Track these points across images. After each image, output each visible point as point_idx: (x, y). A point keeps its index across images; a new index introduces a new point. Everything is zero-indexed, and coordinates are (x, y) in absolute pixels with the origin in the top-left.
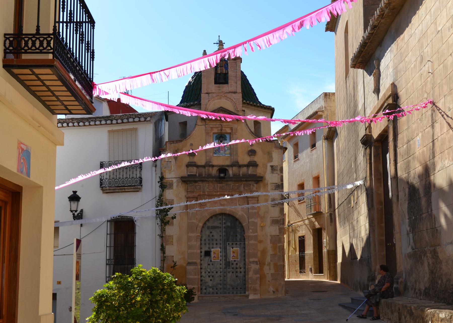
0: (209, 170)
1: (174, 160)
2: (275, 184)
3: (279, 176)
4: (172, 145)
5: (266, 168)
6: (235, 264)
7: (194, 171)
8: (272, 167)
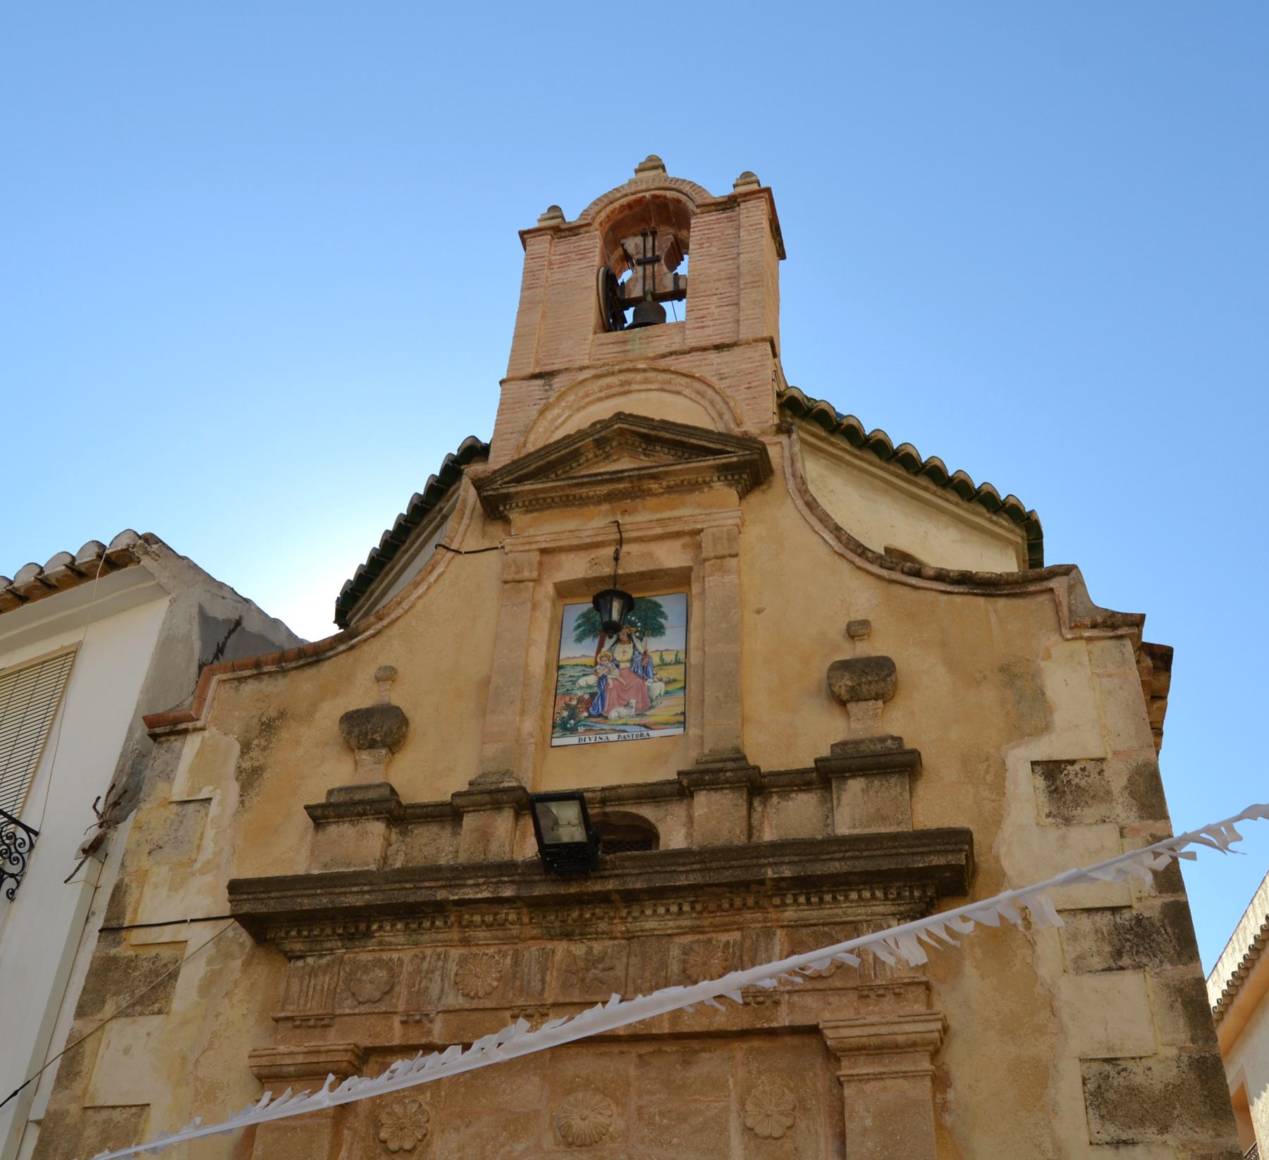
0: (485, 836)
1: (235, 787)
2: (1104, 921)
4: (250, 688)
5: (999, 787)
8: (1051, 770)
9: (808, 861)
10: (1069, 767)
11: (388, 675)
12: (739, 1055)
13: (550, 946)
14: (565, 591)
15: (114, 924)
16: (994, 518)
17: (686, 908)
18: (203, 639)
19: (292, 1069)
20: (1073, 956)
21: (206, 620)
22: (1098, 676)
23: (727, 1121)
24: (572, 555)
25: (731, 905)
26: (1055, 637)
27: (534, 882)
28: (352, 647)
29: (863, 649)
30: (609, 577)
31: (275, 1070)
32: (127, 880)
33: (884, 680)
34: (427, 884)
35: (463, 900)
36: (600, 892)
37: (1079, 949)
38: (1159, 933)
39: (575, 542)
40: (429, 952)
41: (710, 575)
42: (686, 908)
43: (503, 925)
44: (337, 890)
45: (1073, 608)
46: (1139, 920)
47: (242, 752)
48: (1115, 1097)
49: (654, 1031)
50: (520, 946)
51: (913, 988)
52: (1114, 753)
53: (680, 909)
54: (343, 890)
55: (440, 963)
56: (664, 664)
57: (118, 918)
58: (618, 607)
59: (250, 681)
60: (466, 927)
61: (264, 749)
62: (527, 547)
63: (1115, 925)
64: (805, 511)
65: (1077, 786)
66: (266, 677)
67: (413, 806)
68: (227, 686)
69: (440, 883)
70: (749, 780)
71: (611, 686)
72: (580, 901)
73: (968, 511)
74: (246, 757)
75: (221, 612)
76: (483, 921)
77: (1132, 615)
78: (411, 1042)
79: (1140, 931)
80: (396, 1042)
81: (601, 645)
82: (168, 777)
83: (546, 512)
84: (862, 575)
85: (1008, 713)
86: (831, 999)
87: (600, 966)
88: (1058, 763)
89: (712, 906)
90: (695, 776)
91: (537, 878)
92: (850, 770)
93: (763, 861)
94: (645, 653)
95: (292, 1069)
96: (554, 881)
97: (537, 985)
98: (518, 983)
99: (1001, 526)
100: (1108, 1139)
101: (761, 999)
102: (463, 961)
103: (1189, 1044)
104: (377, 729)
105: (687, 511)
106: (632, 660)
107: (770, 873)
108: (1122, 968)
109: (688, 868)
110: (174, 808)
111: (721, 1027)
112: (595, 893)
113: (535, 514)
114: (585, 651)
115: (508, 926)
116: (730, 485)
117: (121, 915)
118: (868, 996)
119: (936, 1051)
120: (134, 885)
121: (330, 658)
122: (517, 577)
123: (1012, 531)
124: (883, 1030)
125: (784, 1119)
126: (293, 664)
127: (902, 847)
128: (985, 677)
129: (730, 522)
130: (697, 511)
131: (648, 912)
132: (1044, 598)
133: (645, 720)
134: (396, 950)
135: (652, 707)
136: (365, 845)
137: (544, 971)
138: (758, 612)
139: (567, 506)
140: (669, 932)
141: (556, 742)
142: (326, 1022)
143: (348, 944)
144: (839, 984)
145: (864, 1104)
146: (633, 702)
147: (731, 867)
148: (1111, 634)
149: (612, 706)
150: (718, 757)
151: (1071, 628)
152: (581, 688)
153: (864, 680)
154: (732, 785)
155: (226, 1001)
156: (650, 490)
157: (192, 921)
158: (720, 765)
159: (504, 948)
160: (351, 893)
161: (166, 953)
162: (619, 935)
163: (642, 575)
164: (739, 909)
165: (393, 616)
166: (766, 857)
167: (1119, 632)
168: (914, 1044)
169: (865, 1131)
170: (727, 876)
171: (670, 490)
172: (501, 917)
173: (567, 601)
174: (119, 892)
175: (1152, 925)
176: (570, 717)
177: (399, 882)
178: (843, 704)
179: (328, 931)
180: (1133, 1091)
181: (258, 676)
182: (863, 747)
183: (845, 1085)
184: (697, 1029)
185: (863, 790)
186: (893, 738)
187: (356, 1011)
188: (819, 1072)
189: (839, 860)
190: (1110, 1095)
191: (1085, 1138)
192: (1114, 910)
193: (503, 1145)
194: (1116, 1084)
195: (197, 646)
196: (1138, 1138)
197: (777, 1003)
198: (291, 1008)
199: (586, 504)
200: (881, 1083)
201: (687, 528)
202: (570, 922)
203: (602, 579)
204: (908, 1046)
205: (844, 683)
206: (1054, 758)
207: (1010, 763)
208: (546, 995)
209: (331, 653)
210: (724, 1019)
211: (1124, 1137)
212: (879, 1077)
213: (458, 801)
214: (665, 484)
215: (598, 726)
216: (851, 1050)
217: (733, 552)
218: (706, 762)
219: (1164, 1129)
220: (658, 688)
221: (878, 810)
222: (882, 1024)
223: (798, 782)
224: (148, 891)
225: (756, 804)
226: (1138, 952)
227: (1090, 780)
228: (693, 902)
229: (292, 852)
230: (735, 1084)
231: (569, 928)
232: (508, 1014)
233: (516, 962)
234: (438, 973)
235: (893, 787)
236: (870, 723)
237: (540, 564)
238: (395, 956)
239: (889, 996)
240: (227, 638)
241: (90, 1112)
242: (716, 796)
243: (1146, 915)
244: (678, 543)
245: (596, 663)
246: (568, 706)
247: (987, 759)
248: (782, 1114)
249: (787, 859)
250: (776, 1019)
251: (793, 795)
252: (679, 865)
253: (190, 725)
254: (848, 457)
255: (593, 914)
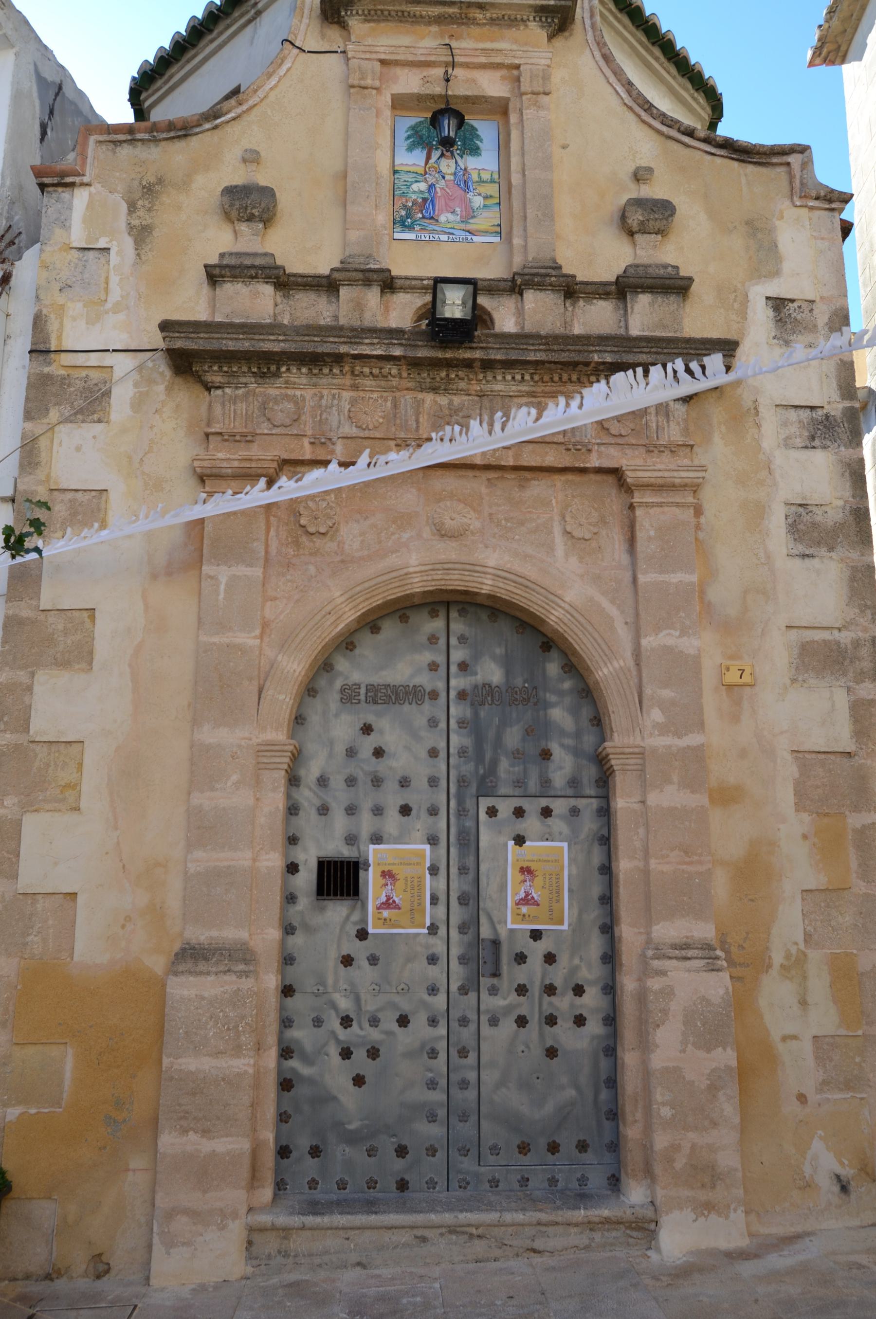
0: (359, 307)
1: (129, 242)
2: (805, 414)
3: (830, 367)
4: (125, 151)
6: (535, 961)
7: (257, 302)
8: (778, 304)
9: (624, 352)
10: (790, 304)
11: (252, 158)
12: (559, 484)
13: (420, 396)
14: (400, 103)
15: (42, 347)
16: (696, 95)
17: (527, 377)
18: (41, 98)
19: (229, 471)
20: (784, 437)
21: (41, 80)
22: (815, 238)
23: (552, 526)
24: (406, 70)
25: (560, 378)
26: (787, 203)
27: (418, 346)
28: (216, 127)
29: (647, 191)
30: (440, 96)
31: (214, 471)
32: (45, 311)
33: (667, 219)
34: (332, 339)
35: (391, 356)
36: (469, 359)
37: (787, 432)
38: (839, 426)
39: (411, 58)
40: (325, 392)
41: (528, 108)
42: (527, 377)
43: (387, 377)
44: (257, 337)
45: (805, 181)
46: (827, 417)
47: (129, 211)
48: (804, 528)
49: (503, 463)
50: (398, 394)
51: (683, 448)
52: (821, 298)
53: (523, 378)
54: (262, 337)
55: (336, 402)
56: (481, 181)
57: (45, 343)
58: (445, 125)
59: (125, 145)
60: (357, 376)
61: (149, 210)
62: (368, 56)
63: (812, 418)
64: (602, 63)
65: (795, 319)
66: (139, 144)
67: (294, 275)
68: (104, 147)
69: (342, 340)
70: (568, 286)
71: (439, 194)
72: (449, 364)
73: (680, 85)
74: (134, 215)
75: (50, 76)
76: (371, 373)
77: (845, 193)
78: (319, 458)
79: (828, 424)
80: (308, 456)
81: (428, 158)
82: (65, 224)
83: (382, 25)
84: (646, 128)
85: (750, 258)
86: (627, 451)
87: (461, 414)
88: (783, 300)
89: (546, 378)
90: (527, 277)
91: (420, 343)
92: (641, 287)
93: (592, 348)
94: (465, 169)
95: (229, 471)
96: (433, 347)
97: (412, 424)
98: (398, 421)
99: (698, 103)
100: (798, 553)
101: (579, 447)
102: (353, 402)
103: (851, 499)
104: (249, 204)
105: (507, 44)
106: (455, 174)
107: (596, 358)
108: (814, 447)
109: (537, 348)
110: (76, 254)
111: (551, 464)
112: (464, 360)
113: (372, 24)
114: (414, 160)
115: (390, 378)
116: (542, 27)
117: (46, 340)
118: (653, 451)
119: (695, 488)
120: (52, 316)
121: (197, 134)
122: (363, 83)
123: (704, 109)
124: (666, 474)
125: (592, 528)
126: (164, 135)
127: (691, 349)
128: (735, 227)
129: (543, 62)
130: (514, 47)
131: (499, 378)
132: (782, 170)
133: (469, 227)
134: (298, 389)
135: (474, 217)
136: (257, 302)
137: (417, 414)
138: (564, 147)
139: (401, 21)
140: (511, 394)
141: (397, 236)
142: (249, 438)
143: (260, 381)
144: (634, 442)
145: (648, 523)
146: (458, 210)
147: (568, 350)
148: (827, 206)
149: (441, 212)
150: (541, 264)
151: (801, 197)
152: (415, 192)
153: (648, 217)
154: (554, 288)
155: (157, 416)
156: (475, 19)
157: (113, 351)
158: (543, 271)
159: (385, 394)
160: (269, 340)
161: (95, 375)
162: (473, 393)
163: (467, 98)
164: (566, 382)
165: (251, 103)
166: (593, 345)
167: (834, 206)
168: (686, 485)
169: (650, 538)
170: (564, 357)
171: (493, 21)
172: (385, 371)
173: (398, 113)
174: (39, 322)
175: (835, 420)
176: (409, 216)
177: (308, 336)
178: (631, 234)
179: (245, 369)
180: (815, 525)
181: (133, 141)
182: (650, 270)
183: (637, 508)
184: (534, 464)
185: (649, 303)
186: (673, 266)
187: (274, 432)
188: (614, 499)
189: (646, 353)
190: (801, 527)
191: (785, 551)
192: (812, 408)
193: (393, 534)
194: (805, 520)
195: (37, 103)
196: (815, 554)
197: (590, 451)
198: (218, 426)
199: (417, 23)
200: (661, 509)
201: (508, 61)
202: (438, 379)
203: (433, 98)
204: (681, 486)
205: (635, 218)
206: (781, 297)
207: (751, 296)
208: (421, 432)
209: (198, 130)
210: (552, 459)
211: (807, 552)
212: (660, 505)
213: (336, 275)
214: (488, 15)
215: (431, 227)
216: (642, 486)
217: (547, 91)
218: (531, 267)
219: (831, 549)
220: (478, 201)
221: (661, 320)
222: (666, 470)
223: (601, 291)
224: (68, 323)
225: (567, 305)
226: (825, 438)
227: (804, 316)
228: (532, 374)
229: (193, 303)
230: (557, 503)
231: (437, 384)
232: (392, 443)
233: (395, 406)
234: (334, 409)
235: (668, 304)
236: (651, 252)
237: (381, 73)
238: (298, 393)
239: (667, 452)
240: (55, 100)
241: (56, 493)
242: (540, 295)
243: (832, 414)
244: (498, 74)
245: (426, 173)
246: (405, 207)
247: (735, 291)
248: (590, 524)
249: (609, 349)
250: (589, 462)
251: (595, 301)
252: (529, 344)
253: (77, 180)
254: (611, 18)
255: (457, 376)
